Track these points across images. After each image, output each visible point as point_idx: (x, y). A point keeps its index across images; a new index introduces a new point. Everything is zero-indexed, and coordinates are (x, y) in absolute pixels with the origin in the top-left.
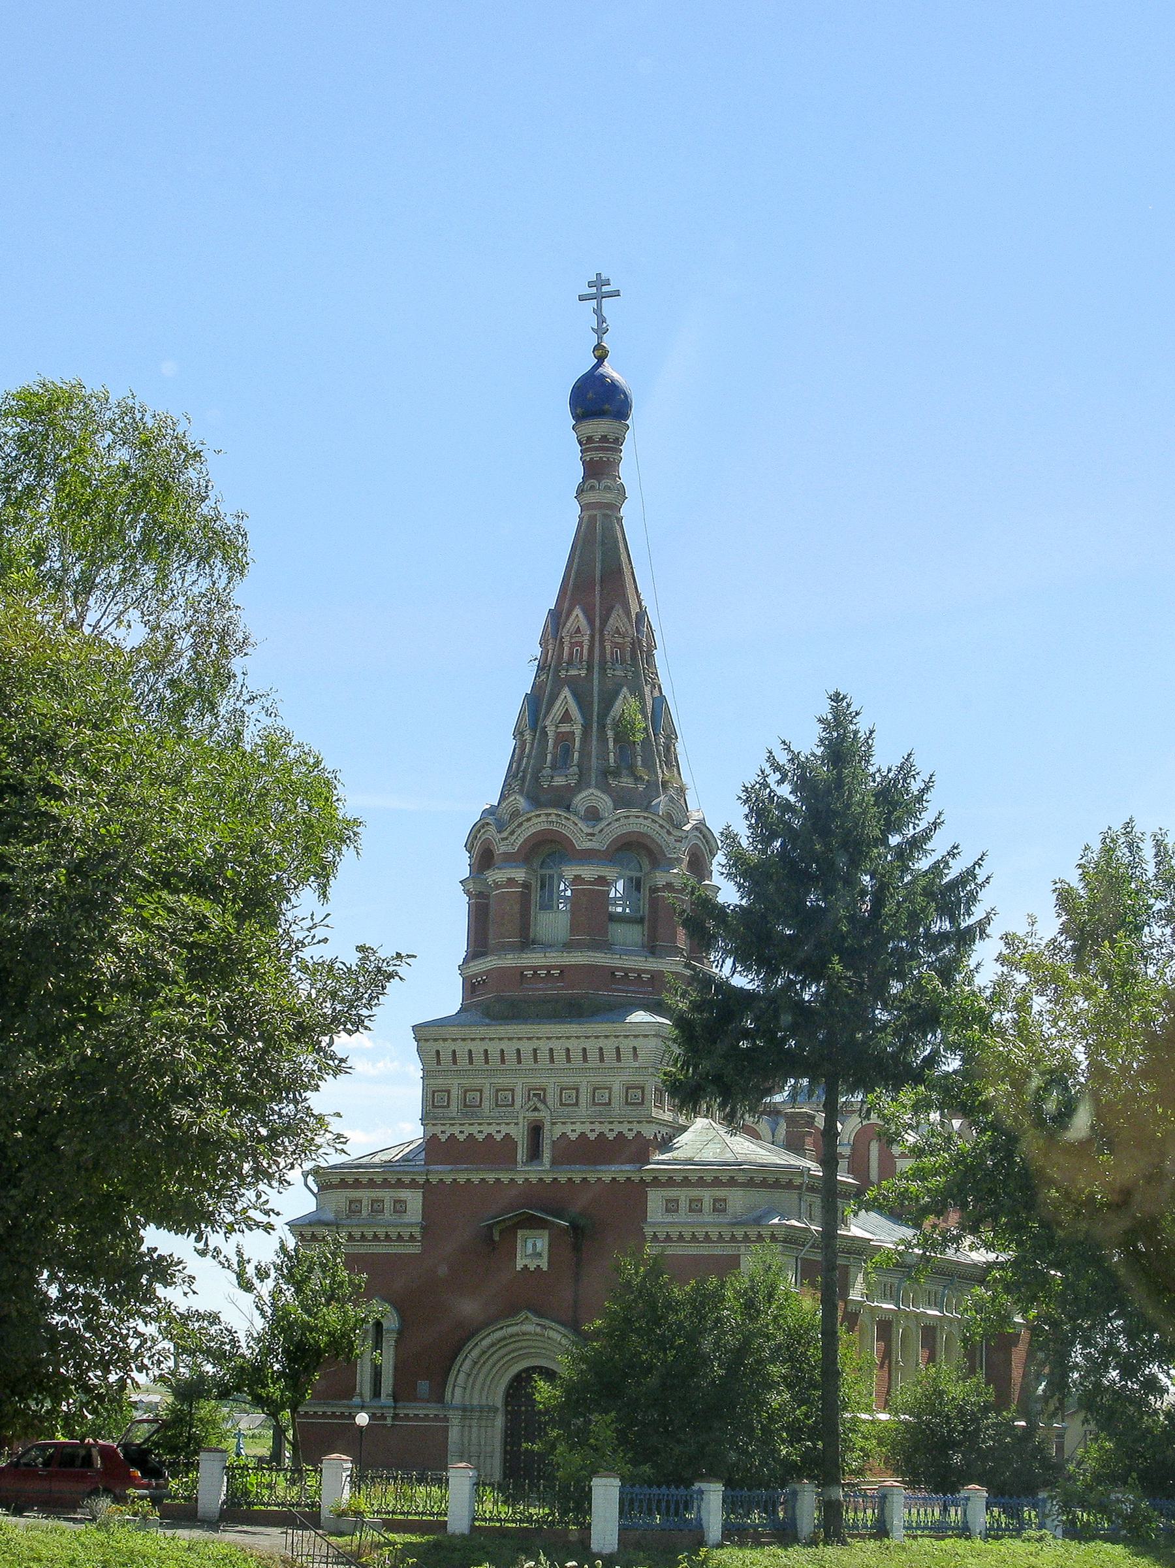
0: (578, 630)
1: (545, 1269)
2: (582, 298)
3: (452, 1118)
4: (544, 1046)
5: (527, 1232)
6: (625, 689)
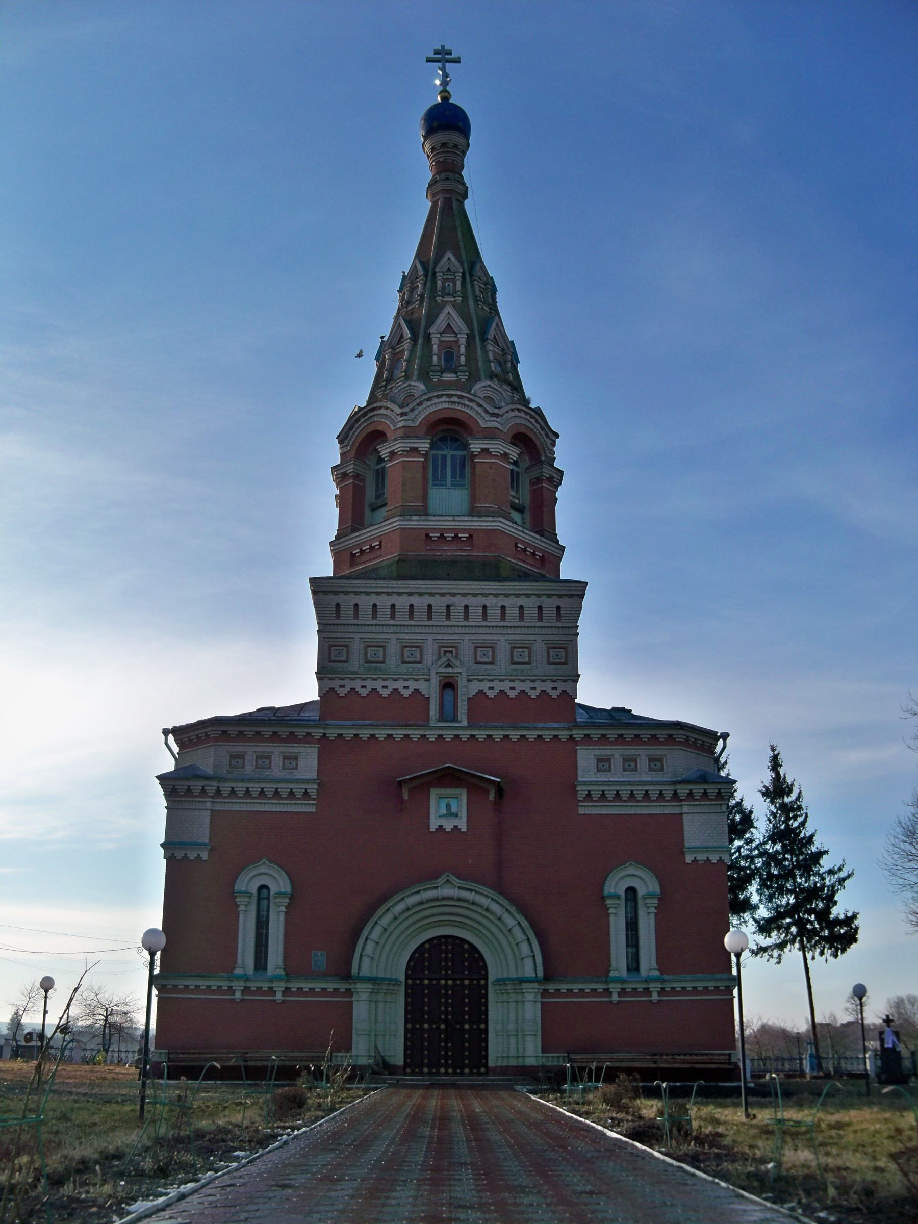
1: (464, 829)
3: (353, 673)
4: (460, 602)
5: (442, 791)
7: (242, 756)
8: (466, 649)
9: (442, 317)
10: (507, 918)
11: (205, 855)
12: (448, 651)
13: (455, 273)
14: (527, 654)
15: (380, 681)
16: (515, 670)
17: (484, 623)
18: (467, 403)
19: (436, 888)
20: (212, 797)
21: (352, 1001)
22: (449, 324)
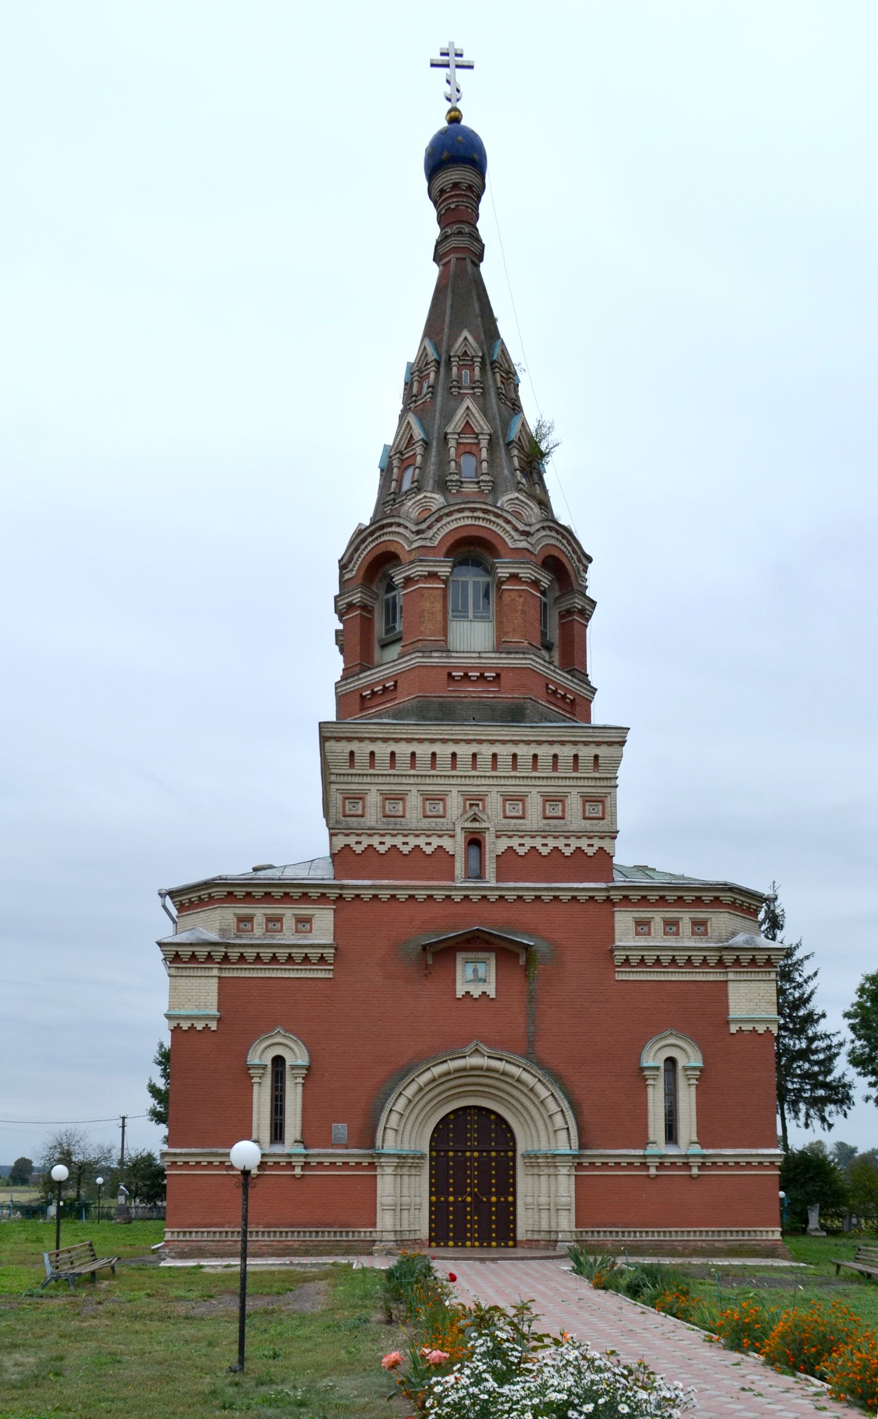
1: (493, 996)
4: (486, 751)
5: (470, 955)
7: (249, 919)
8: (494, 802)
9: (461, 411)
10: (540, 1088)
11: (213, 1026)
12: (474, 801)
13: (473, 357)
14: (560, 807)
16: (548, 825)
17: (513, 774)
18: (493, 519)
19: (465, 1057)
20: (219, 963)
21: (376, 1175)
22: (467, 422)
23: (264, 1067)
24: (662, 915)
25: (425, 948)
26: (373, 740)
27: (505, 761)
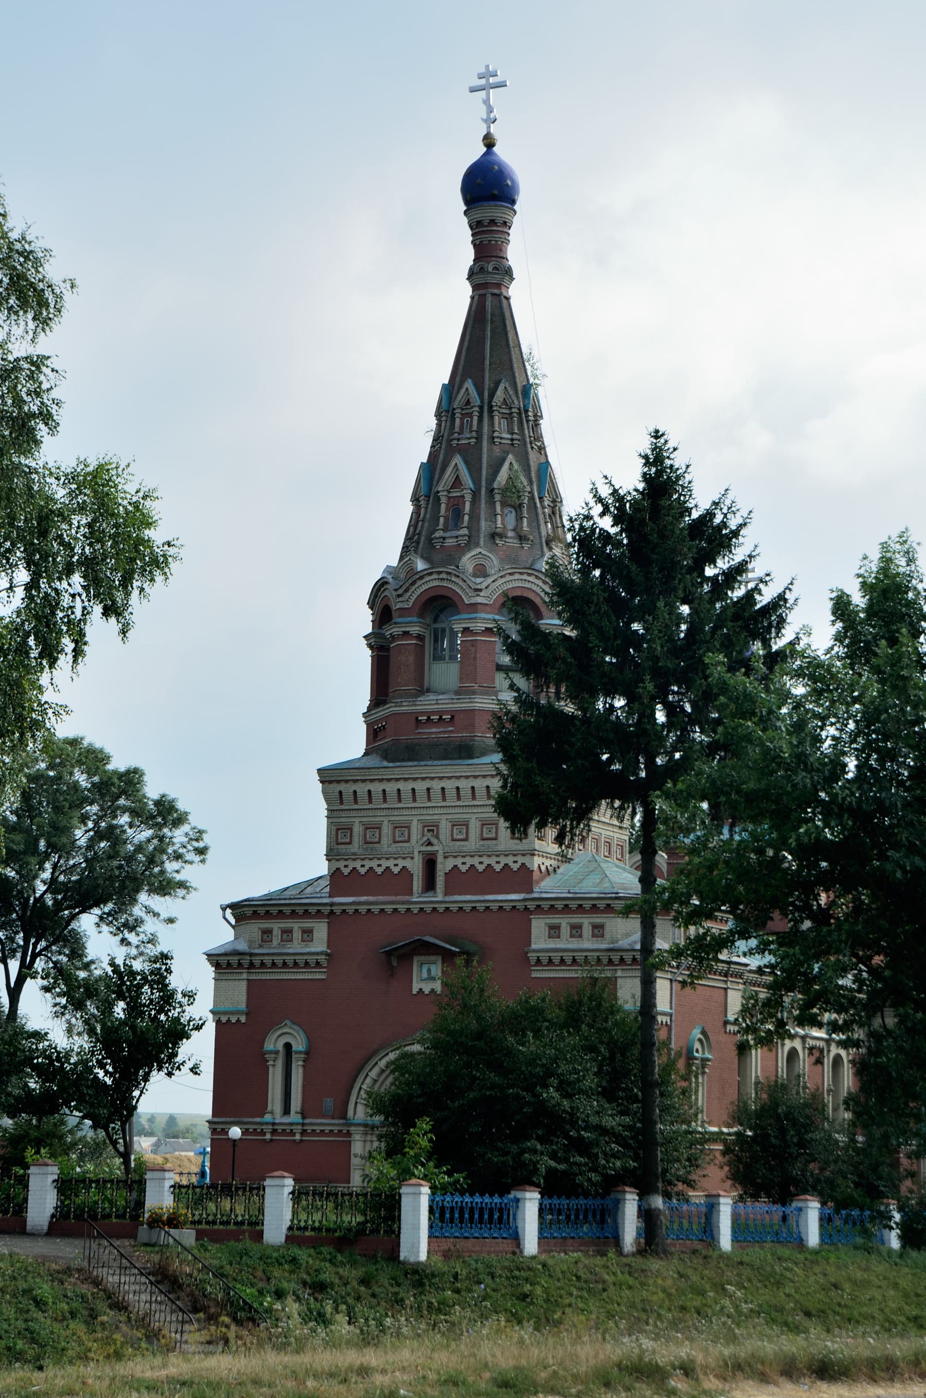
0: (468, 402)
2: (473, 90)
3: (354, 854)
4: (436, 786)
5: (423, 958)
6: (510, 457)
8: (445, 828)
11: (243, 1019)
12: (432, 828)
15: (375, 860)
16: (483, 846)
17: (458, 803)
18: (454, 579)
20: (248, 968)
23: (277, 1052)
24: (567, 920)
25: (388, 954)
26: (355, 781)
27: (451, 793)
